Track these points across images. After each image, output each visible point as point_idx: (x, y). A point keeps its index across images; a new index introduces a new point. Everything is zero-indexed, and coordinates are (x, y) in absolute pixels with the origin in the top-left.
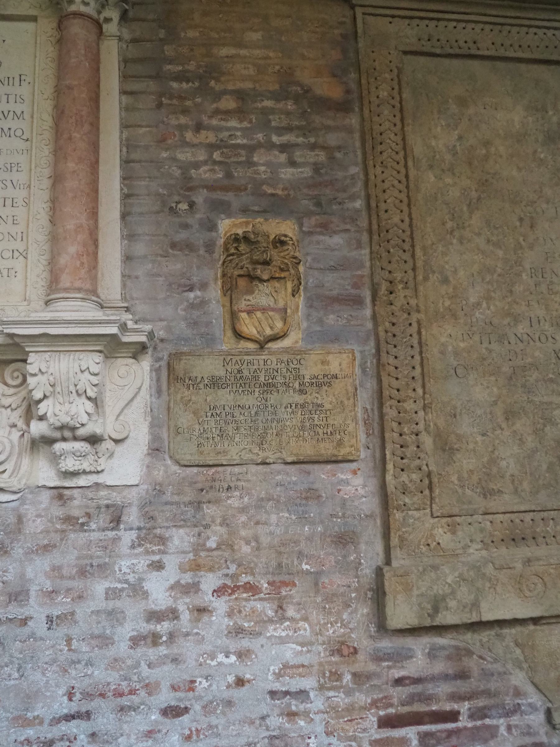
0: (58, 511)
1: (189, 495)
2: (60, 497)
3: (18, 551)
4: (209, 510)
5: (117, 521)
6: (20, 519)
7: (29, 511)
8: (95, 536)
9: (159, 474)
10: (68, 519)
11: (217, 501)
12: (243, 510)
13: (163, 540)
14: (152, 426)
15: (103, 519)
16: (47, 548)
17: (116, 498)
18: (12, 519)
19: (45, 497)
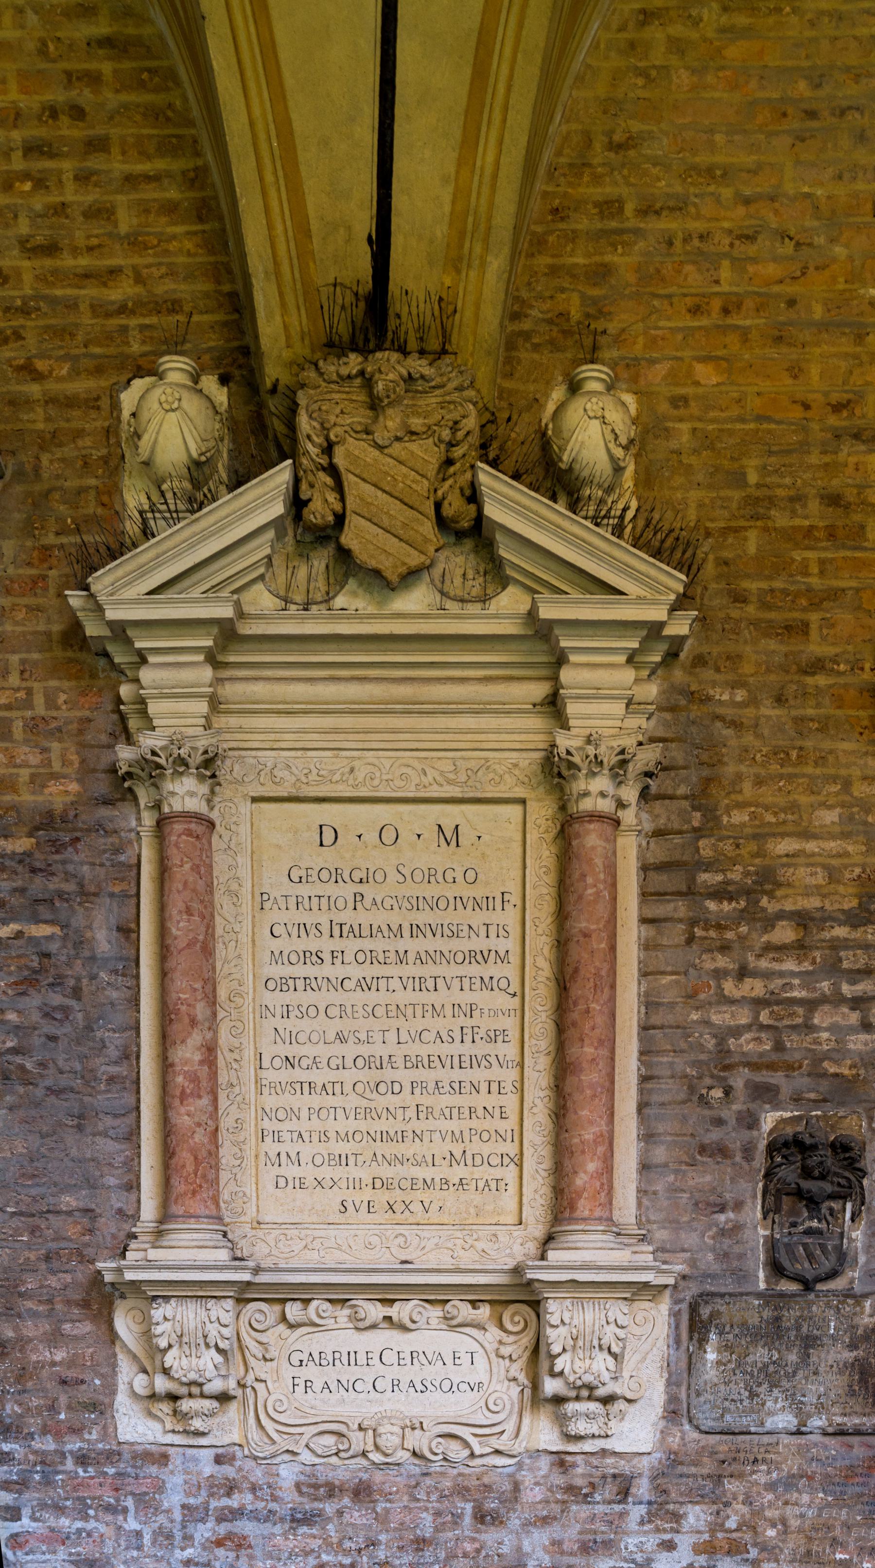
0: (559, 1480)
1: (708, 1467)
2: (562, 1464)
3: (515, 1522)
4: (731, 1486)
5: (624, 1493)
6: (517, 1487)
7: (527, 1478)
8: (600, 1509)
9: (674, 1441)
10: (570, 1489)
11: (740, 1476)
12: (771, 1487)
13: (677, 1517)
14: (669, 1383)
15: (609, 1491)
16: (545, 1521)
17: (624, 1467)
18: (507, 1486)
19: (544, 1463)
